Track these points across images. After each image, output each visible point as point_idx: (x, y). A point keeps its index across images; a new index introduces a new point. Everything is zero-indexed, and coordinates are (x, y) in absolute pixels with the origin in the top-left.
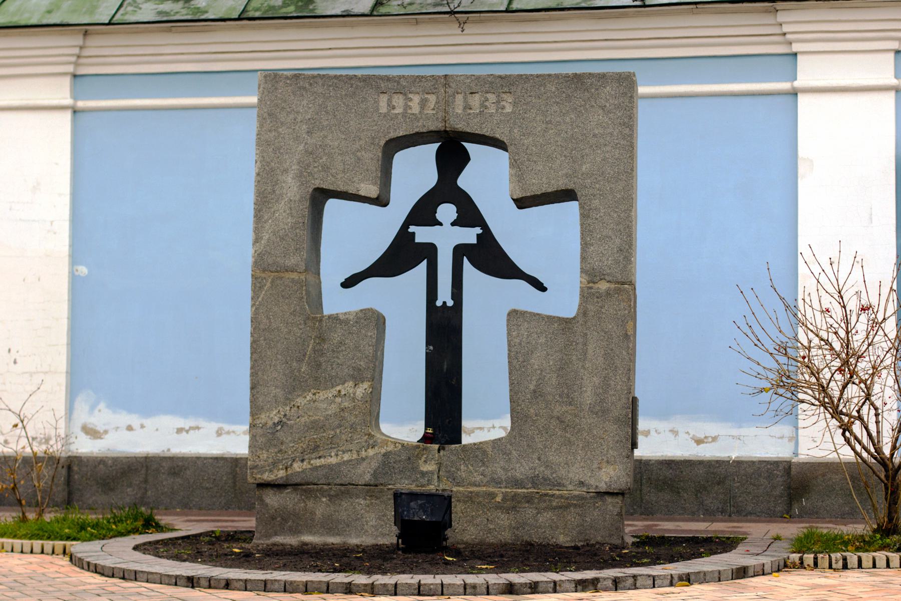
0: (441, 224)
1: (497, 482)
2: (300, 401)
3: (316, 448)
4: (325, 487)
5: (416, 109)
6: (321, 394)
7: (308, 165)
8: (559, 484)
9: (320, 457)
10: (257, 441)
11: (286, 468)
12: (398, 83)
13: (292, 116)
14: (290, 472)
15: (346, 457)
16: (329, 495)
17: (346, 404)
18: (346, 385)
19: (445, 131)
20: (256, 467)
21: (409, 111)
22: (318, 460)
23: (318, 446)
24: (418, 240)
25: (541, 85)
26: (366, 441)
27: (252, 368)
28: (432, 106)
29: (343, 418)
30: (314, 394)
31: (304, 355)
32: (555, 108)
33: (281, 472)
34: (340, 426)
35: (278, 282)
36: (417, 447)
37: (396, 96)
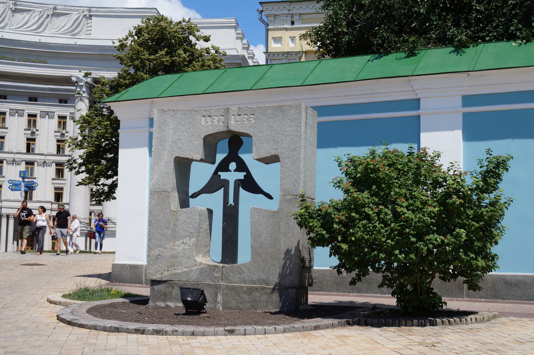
1: (245, 282)
2: (167, 246)
5: (216, 123)
12: (210, 112)
14: (163, 275)
15: (186, 270)
20: (150, 273)
24: (222, 177)
32: (271, 120)
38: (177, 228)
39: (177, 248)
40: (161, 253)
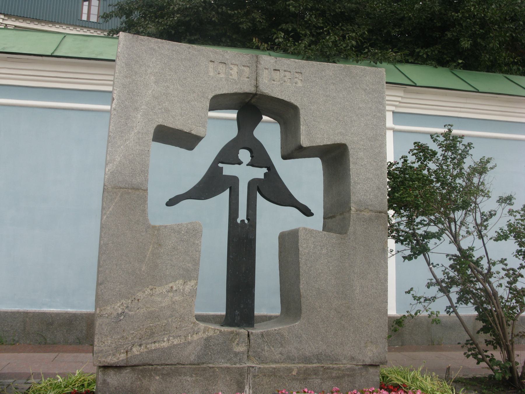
0: (240, 163)
2: (140, 295)
4: (159, 367)
5: (235, 76)
6: (157, 290)
9: (155, 342)
10: (103, 329)
11: (127, 352)
14: (129, 355)
16: (162, 374)
17: (177, 298)
18: (177, 282)
19: (256, 94)
21: (230, 77)
25: (323, 71)
26: (192, 328)
28: (247, 76)
30: (151, 290)
33: (122, 355)
36: (232, 332)
37: (221, 65)
39: (160, 299)
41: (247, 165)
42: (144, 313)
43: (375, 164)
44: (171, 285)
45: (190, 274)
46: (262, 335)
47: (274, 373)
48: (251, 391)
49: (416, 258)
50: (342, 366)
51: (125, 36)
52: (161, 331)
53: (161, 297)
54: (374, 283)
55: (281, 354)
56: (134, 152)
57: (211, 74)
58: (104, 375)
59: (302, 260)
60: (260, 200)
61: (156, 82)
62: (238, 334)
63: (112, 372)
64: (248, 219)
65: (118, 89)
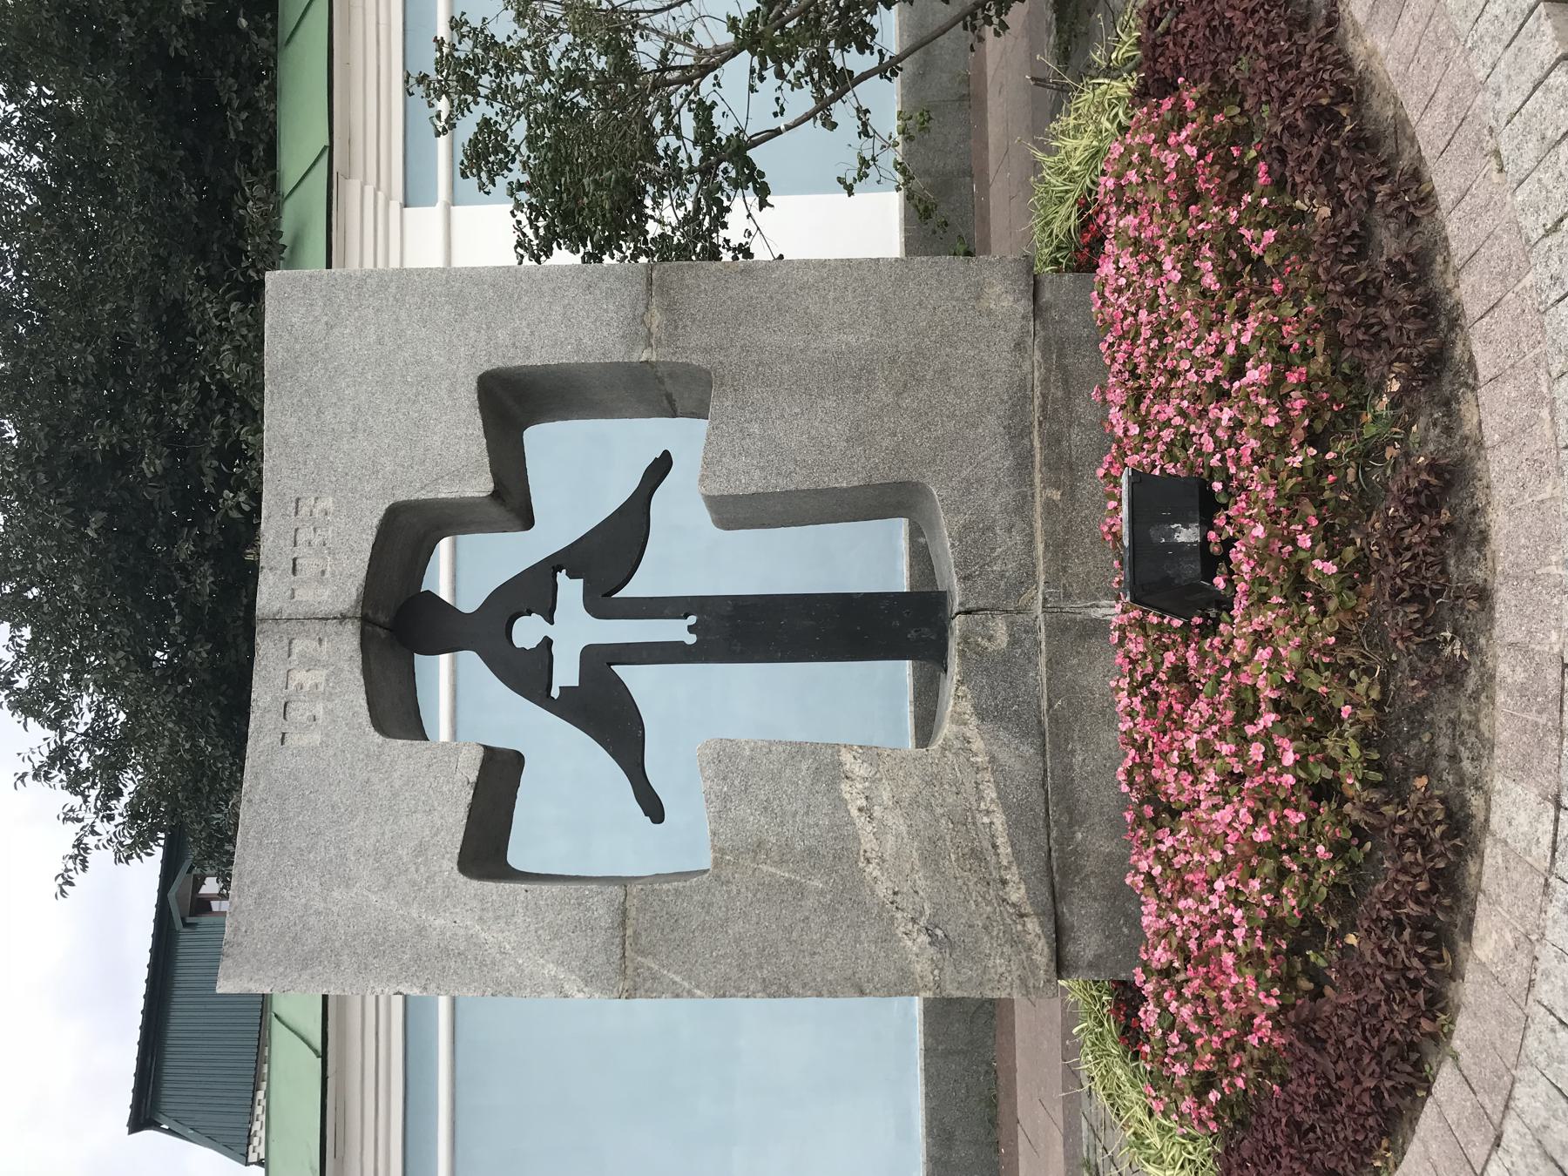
0: (547, 643)
1: (1022, 506)
2: (882, 891)
3: (976, 854)
4: (1054, 834)
5: (319, 676)
7: (414, 884)
8: (1022, 387)
9: (995, 846)
10: (970, 979)
11: (1022, 916)
13: (312, 920)
14: (1028, 909)
15: (991, 793)
16: (1070, 825)
17: (886, 795)
18: (847, 796)
19: (365, 620)
21: (321, 688)
22: (1001, 850)
23: (972, 850)
25: (286, 443)
27: (820, 995)
28: (316, 644)
29: (914, 801)
30: (868, 861)
31: (791, 882)
32: (328, 416)
33: (1029, 926)
34: (929, 807)
35: (643, 940)
36: (962, 654)
37: (292, 714)
38: (799, 846)
39: (891, 839)
40: (923, 922)
41: (552, 623)
42: (926, 878)
43: (526, 299)
44: (854, 812)
45: (825, 766)
46: (966, 578)
47: (1058, 548)
48: (1104, 602)
49: (762, 174)
50: (1036, 374)
51: (228, 978)
52: (968, 831)
53: (884, 836)
54: (831, 295)
55: (1009, 530)
56: (532, 928)
57: (317, 738)
58: (1076, 969)
59: (783, 484)
60: (635, 589)
61: (347, 886)
62: (965, 639)
63: (1071, 949)
64: (686, 617)
65: (372, 983)
